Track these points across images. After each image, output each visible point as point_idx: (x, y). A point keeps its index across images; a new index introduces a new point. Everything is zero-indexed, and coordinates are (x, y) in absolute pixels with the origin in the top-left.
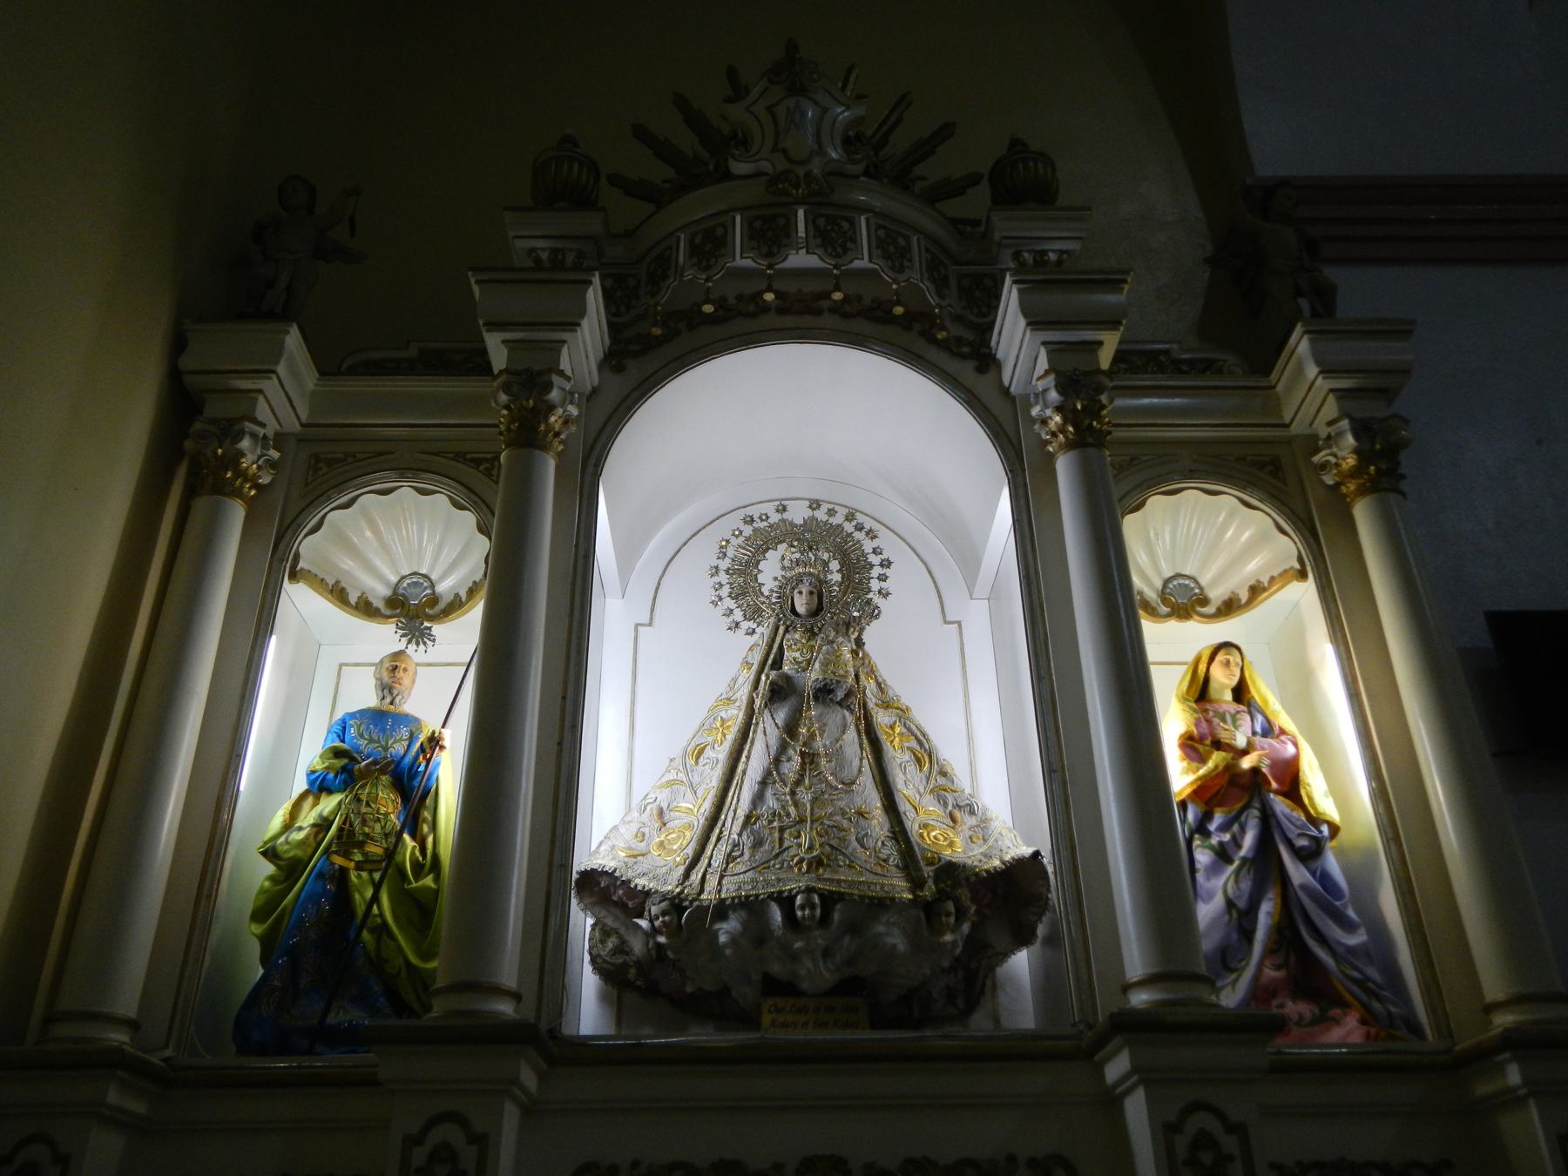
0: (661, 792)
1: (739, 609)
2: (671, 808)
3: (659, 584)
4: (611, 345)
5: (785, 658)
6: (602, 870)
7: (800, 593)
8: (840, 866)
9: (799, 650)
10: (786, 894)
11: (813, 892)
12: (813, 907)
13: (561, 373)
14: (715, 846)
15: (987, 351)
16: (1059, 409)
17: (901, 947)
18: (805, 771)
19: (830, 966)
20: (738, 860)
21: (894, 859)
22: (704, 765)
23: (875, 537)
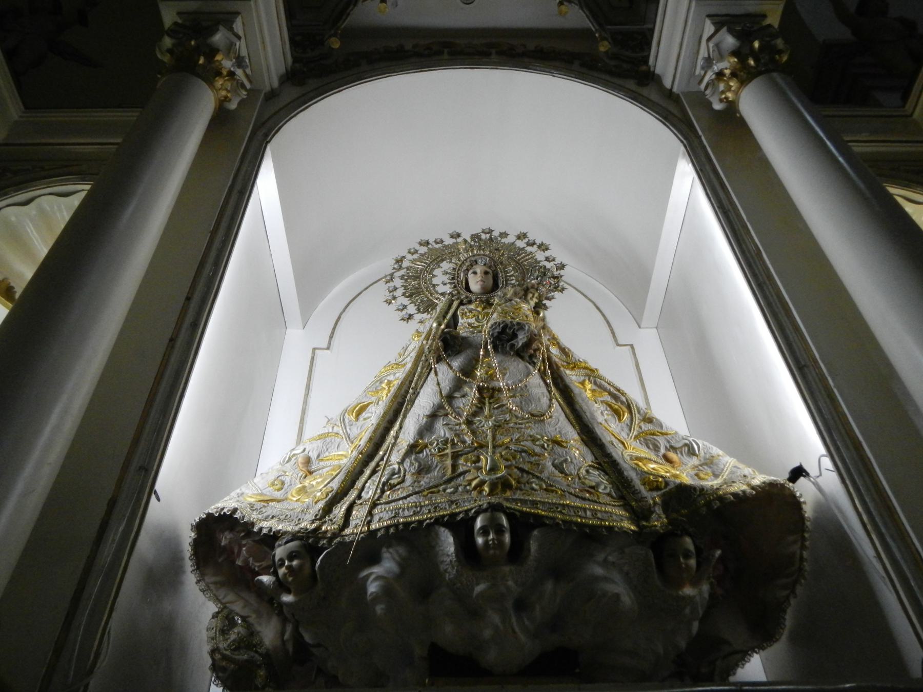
1: (413, 305)
2: (320, 458)
3: (339, 318)
5: (459, 324)
6: (220, 514)
7: (475, 273)
8: (533, 489)
9: (474, 316)
10: (461, 515)
11: (498, 510)
12: (499, 530)
13: (231, 29)
14: (369, 477)
15: (644, 68)
16: (735, 53)
17: (627, 599)
19: (527, 622)
20: (398, 487)
21: (606, 488)
23: (547, 249)
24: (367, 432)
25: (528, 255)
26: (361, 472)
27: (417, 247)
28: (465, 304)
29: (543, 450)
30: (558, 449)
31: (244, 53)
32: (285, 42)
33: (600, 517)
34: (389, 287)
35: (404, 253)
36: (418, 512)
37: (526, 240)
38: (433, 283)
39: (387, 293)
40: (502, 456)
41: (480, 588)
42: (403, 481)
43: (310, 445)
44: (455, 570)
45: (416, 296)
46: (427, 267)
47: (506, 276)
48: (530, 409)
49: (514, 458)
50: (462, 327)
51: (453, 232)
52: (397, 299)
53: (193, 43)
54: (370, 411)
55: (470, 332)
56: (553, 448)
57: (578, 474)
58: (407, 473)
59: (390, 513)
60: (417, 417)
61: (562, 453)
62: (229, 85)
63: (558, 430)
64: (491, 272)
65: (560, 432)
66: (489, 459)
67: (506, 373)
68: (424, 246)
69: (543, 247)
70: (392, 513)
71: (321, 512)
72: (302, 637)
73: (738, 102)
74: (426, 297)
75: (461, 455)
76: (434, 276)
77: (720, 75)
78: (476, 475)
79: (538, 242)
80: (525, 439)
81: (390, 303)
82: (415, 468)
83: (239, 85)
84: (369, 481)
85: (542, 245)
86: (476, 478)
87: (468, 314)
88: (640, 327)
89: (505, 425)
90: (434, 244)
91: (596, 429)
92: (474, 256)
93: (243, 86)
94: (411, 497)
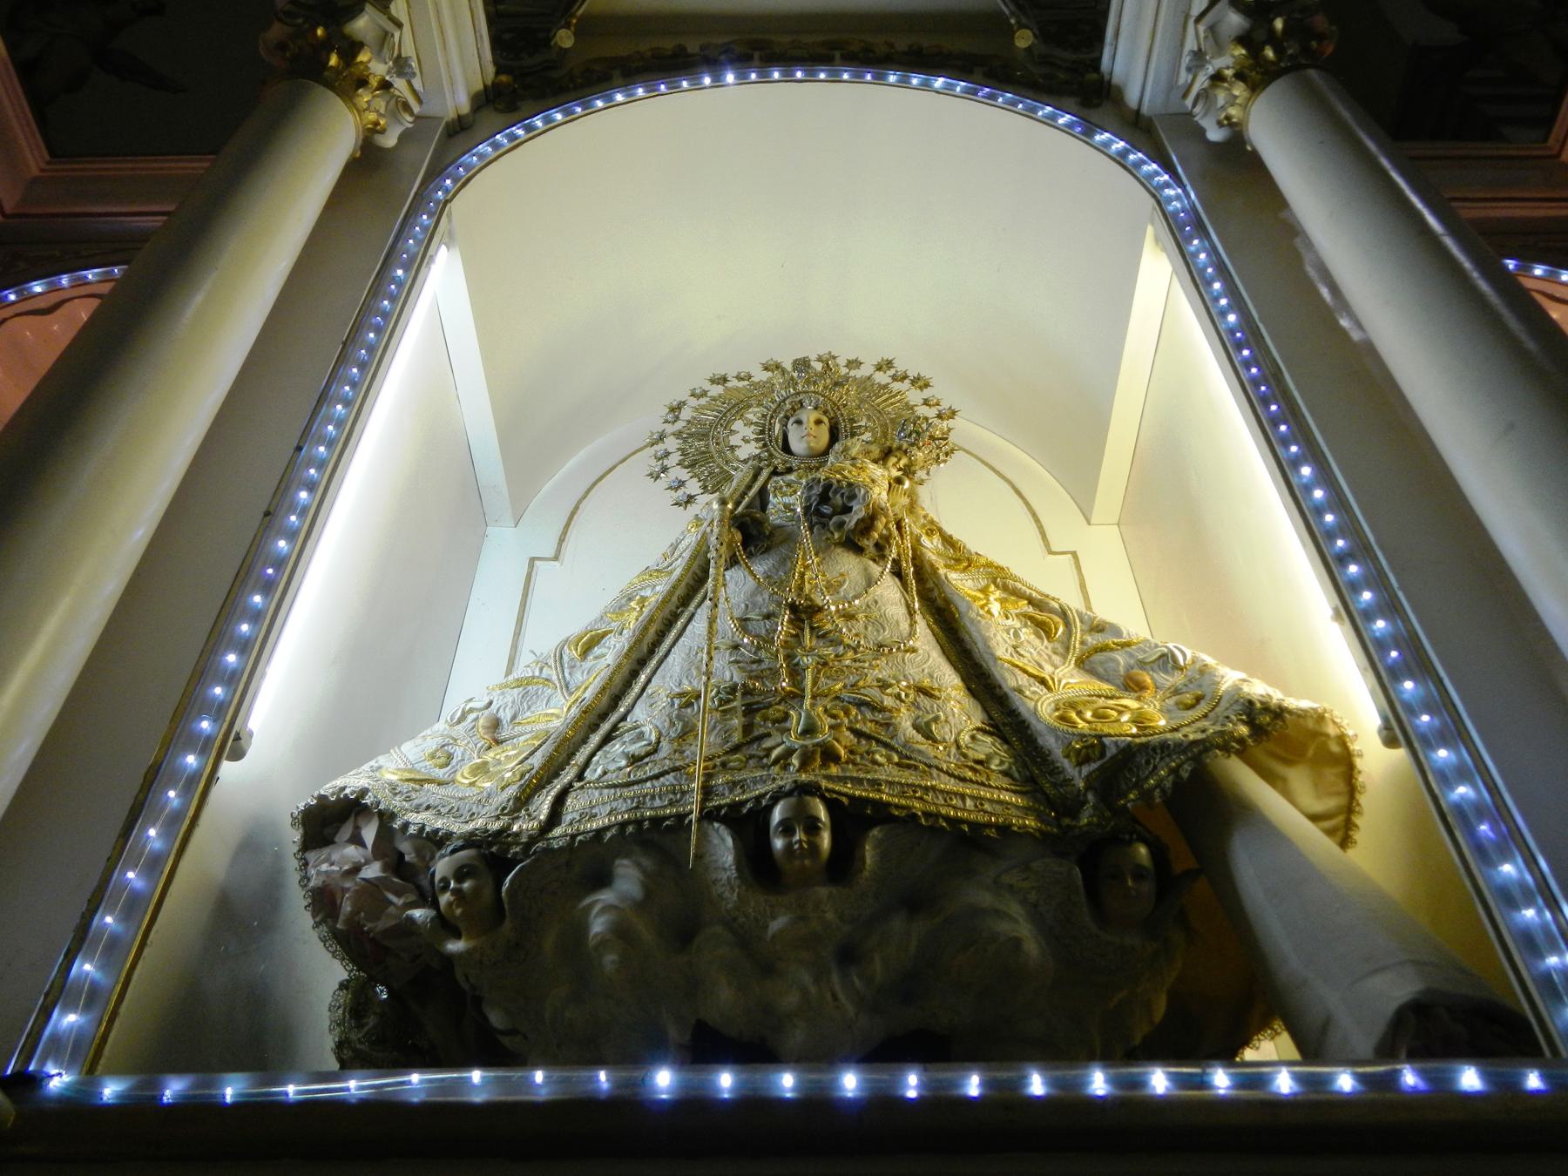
0: (503, 693)
1: (696, 479)
3: (577, 508)
4: (497, 73)
5: (770, 506)
7: (799, 422)
8: (875, 762)
10: (749, 805)
11: (812, 794)
12: (812, 826)
14: (600, 747)
16: (1242, 40)
18: (802, 630)
20: (646, 760)
21: (1002, 763)
22: (596, 658)
23: (927, 385)
24: (598, 678)
25: (895, 396)
26: (585, 741)
27: (707, 386)
28: (782, 474)
29: (898, 702)
30: (922, 699)
31: (408, 50)
32: (481, 36)
33: (989, 810)
34: (656, 452)
35: (683, 395)
36: (677, 801)
37: (892, 372)
38: (731, 444)
39: (653, 462)
40: (826, 711)
41: (776, 925)
42: (655, 751)
43: (501, 697)
44: (735, 895)
45: (702, 466)
46: (722, 418)
47: (852, 428)
48: (881, 638)
49: (847, 713)
50: (773, 511)
51: (767, 362)
52: (670, 470)
53: (320, 32)
54: (607, 645)
55: (787, 517)
56: (915, 700)
57: (956, 741)
58: (662, 739)
59: (629, 801)
60: (687, 652)
61: (932, 707)
62: (383, 104)
63: (926, 671)
64: (826, 420)
65: (931, 676)
66: (803, 714)
67: (844, 581)
68: (718, 384)
69: (921, 383)
70: (632, 803)
71: (511, 803)
72: (485, 1019)
73: (1248, 122)
74: (718, 466)
75: (758, 710)
76: (733, 432)
77: (1217, 78)
78: (779, 740)
79: (912, 374)
80: (868, 684)
81: (658, 477)
82: (676, 730)
83: (399, 104)
84: (599, 753)
85: (919, 379)
86: (779, 745)
87: (784, 489)
88: (1089, 524)
89: (836, 663)
90: (735, 381)
91: (993, 669)
92: (798, 394)
93: (406, 107)
94: (667, 776)
